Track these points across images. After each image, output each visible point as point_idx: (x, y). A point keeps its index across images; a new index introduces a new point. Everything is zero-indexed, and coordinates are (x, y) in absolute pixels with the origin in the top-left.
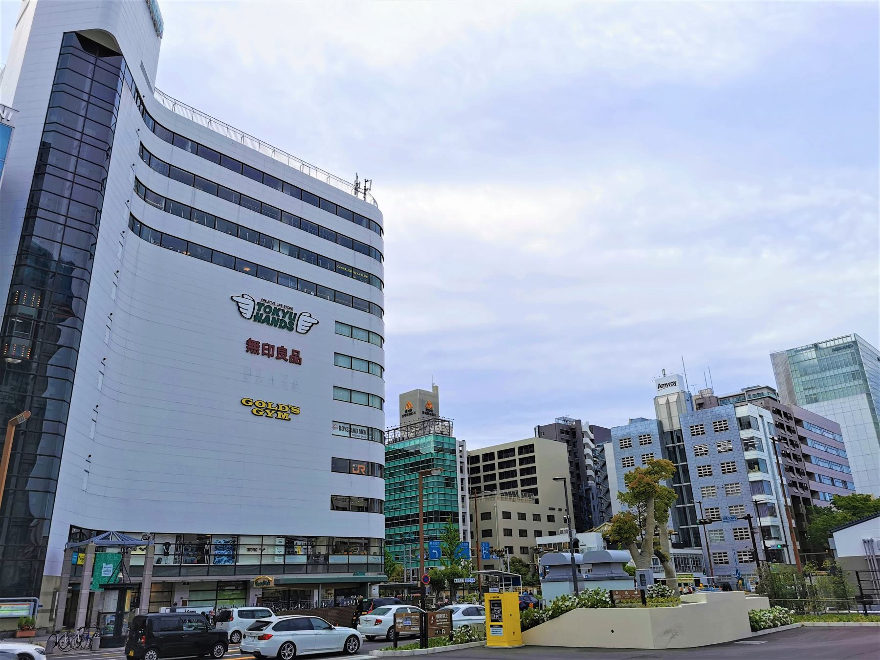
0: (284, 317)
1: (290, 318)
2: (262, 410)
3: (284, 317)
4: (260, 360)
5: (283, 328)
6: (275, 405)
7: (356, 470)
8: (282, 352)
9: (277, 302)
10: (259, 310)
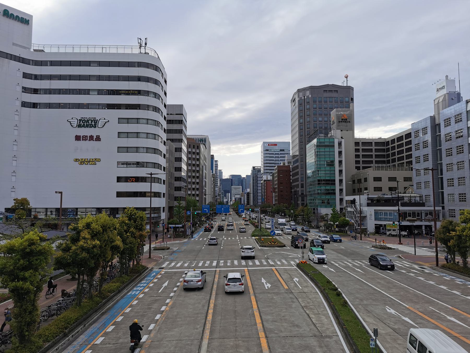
0: (91, 122)
4: (82, 142)
5: (91, 127)
7: (130, 180)
8: (91, 138)
9: (88, 117)
10: (80, 122)
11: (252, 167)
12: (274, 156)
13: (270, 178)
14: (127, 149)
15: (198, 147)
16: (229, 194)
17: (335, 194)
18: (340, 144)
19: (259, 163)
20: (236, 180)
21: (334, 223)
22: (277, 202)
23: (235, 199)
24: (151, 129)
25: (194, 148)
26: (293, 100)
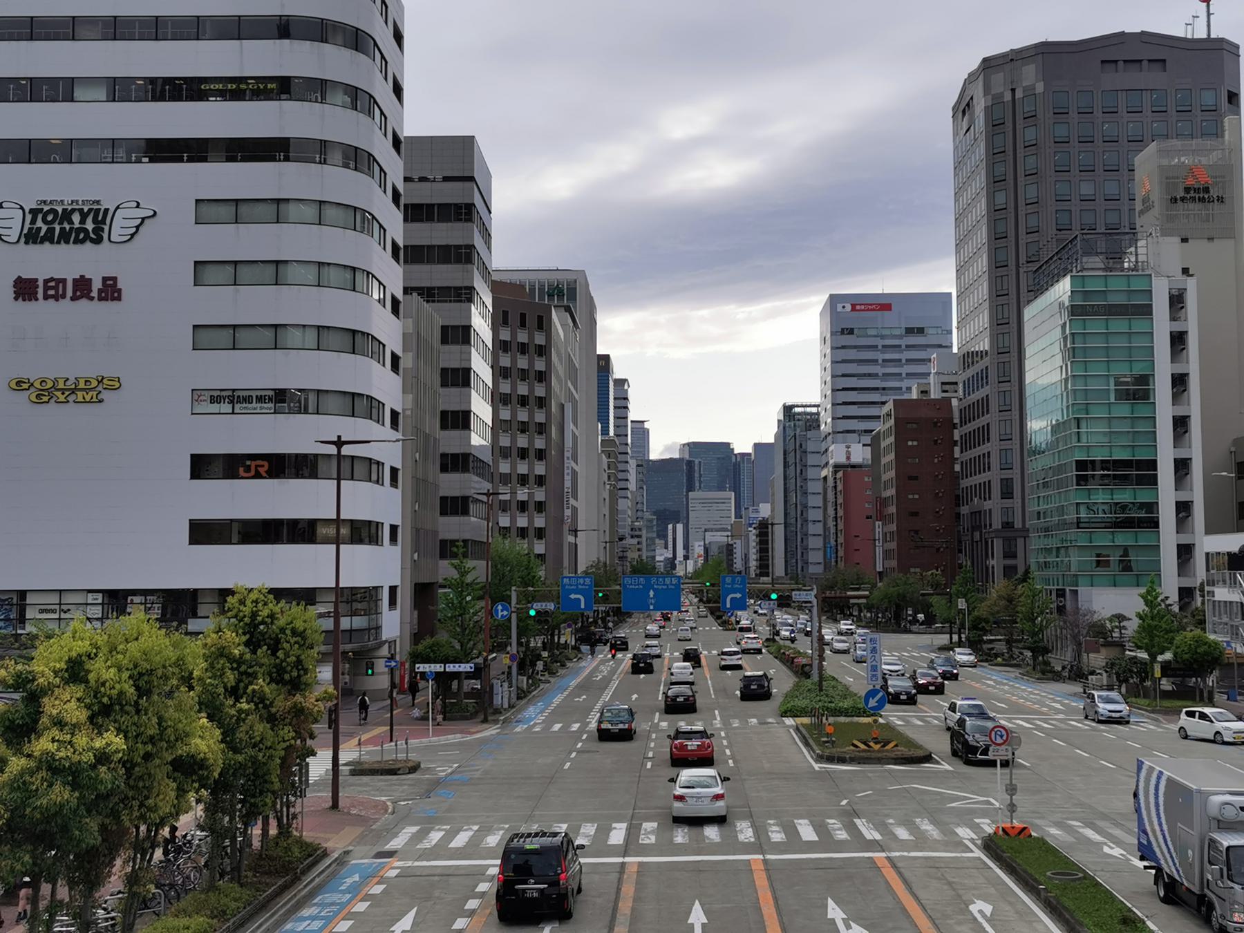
0: (83, 221)
1: (95, 221)
2: (47, 393)
3: (83, 221)
4: (41, 308)
5: (82, 242)
6: (72, 380)
7: (248, 469)
8: (82, 287)
10: (33, 221)
11: (781, 406)
12: (881, 356)
13: (860, 454)
14: (233, 336)
15: (543, 323)
16: (680, 527)
17: (1154, 524)
18: (1177, 301)
19: (809, 387)
20: (709, 464)
21: (1153, 657)
22: (894, 563)
23: (706, 550)
24: (339, 245)
25: (523, 324)
26: (963, 108)
